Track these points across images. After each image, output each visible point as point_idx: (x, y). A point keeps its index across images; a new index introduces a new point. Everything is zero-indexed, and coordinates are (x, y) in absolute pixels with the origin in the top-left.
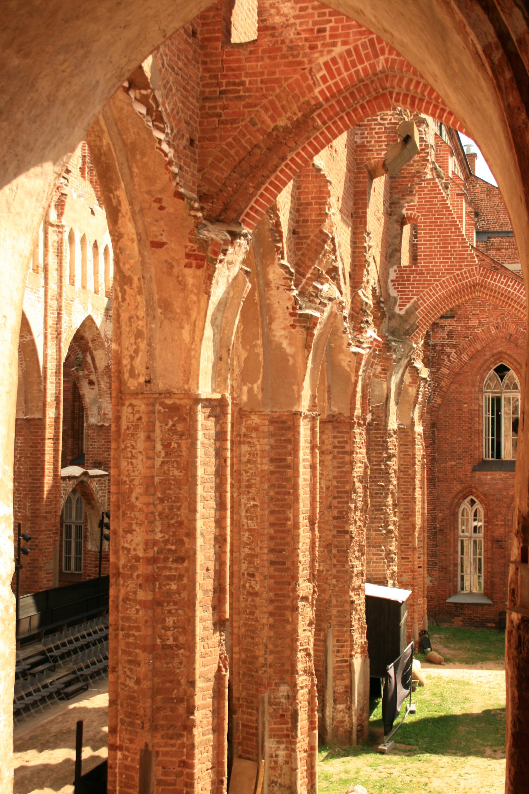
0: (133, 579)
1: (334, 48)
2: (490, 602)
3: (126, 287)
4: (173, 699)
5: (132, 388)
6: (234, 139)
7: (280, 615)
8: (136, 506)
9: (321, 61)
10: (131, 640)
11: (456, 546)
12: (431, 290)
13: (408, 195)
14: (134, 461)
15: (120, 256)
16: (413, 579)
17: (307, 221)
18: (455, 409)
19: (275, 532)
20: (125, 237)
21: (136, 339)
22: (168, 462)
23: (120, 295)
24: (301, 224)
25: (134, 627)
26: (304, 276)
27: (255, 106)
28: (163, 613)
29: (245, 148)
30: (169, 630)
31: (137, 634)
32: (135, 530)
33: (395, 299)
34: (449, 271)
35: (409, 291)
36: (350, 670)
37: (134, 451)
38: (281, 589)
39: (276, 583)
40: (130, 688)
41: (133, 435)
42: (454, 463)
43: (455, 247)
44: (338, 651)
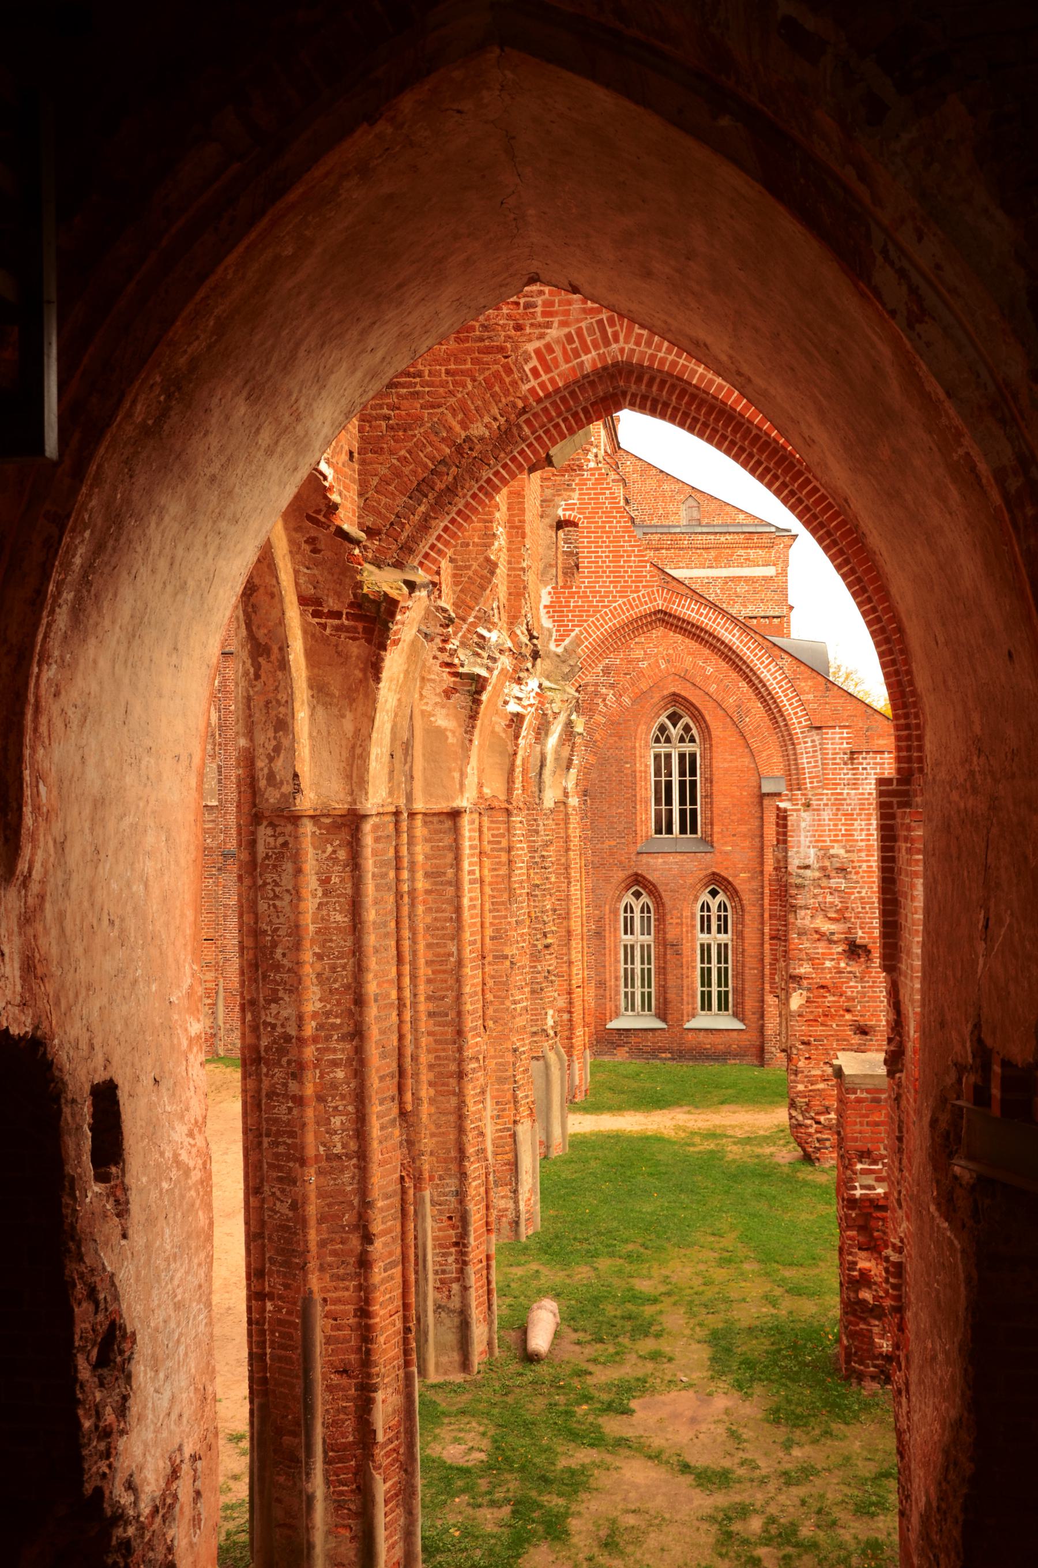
0: (282, 1066)
1: (549, 331)
2: (663, 1025)
3: (260, 659)
4: (343, 1227)
5: (272, 801)
6: (410, 452)
7: (443, 1085)
8: (283, 966)
9: (531, 347)
10: (281, 1149)
11: (617, 953)
12: (597, 619)
13: (565, 490)
14: (278, 903)
15: (253, 616)
16: (570, 1003)
17: (468, 545)
18: (614, 769)
19: (434, 972)
20: (262, 590)
21: (275, 732)
22: (327, 903)
23: (252, 670)
24: (459, 548)
25: (285, 1132)
26: (464, 620)
27: (439, 406)
28: (326, 1112)
29: (426, 466)
30: (336, 1133)
31: (289, 1141)
32: (282, 999)
33: (549, 630)
34: (622, 593)
35: (569, 621)
36: (515, 1141)
37: (277, 889)
38: (444, 1050)
39: (436, 1041)
40: (282, 1215)
41: (275, 866)
42: (614, 843)
43: (629, 561)
44: (499, 1117)
